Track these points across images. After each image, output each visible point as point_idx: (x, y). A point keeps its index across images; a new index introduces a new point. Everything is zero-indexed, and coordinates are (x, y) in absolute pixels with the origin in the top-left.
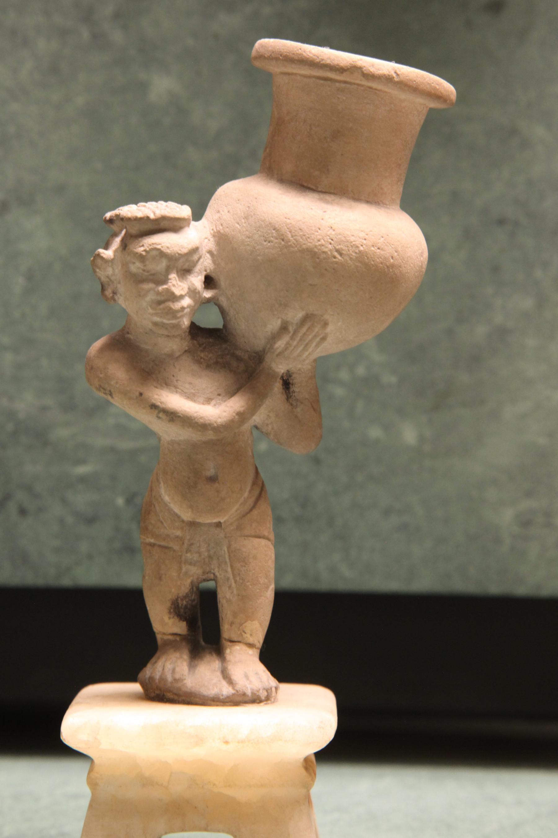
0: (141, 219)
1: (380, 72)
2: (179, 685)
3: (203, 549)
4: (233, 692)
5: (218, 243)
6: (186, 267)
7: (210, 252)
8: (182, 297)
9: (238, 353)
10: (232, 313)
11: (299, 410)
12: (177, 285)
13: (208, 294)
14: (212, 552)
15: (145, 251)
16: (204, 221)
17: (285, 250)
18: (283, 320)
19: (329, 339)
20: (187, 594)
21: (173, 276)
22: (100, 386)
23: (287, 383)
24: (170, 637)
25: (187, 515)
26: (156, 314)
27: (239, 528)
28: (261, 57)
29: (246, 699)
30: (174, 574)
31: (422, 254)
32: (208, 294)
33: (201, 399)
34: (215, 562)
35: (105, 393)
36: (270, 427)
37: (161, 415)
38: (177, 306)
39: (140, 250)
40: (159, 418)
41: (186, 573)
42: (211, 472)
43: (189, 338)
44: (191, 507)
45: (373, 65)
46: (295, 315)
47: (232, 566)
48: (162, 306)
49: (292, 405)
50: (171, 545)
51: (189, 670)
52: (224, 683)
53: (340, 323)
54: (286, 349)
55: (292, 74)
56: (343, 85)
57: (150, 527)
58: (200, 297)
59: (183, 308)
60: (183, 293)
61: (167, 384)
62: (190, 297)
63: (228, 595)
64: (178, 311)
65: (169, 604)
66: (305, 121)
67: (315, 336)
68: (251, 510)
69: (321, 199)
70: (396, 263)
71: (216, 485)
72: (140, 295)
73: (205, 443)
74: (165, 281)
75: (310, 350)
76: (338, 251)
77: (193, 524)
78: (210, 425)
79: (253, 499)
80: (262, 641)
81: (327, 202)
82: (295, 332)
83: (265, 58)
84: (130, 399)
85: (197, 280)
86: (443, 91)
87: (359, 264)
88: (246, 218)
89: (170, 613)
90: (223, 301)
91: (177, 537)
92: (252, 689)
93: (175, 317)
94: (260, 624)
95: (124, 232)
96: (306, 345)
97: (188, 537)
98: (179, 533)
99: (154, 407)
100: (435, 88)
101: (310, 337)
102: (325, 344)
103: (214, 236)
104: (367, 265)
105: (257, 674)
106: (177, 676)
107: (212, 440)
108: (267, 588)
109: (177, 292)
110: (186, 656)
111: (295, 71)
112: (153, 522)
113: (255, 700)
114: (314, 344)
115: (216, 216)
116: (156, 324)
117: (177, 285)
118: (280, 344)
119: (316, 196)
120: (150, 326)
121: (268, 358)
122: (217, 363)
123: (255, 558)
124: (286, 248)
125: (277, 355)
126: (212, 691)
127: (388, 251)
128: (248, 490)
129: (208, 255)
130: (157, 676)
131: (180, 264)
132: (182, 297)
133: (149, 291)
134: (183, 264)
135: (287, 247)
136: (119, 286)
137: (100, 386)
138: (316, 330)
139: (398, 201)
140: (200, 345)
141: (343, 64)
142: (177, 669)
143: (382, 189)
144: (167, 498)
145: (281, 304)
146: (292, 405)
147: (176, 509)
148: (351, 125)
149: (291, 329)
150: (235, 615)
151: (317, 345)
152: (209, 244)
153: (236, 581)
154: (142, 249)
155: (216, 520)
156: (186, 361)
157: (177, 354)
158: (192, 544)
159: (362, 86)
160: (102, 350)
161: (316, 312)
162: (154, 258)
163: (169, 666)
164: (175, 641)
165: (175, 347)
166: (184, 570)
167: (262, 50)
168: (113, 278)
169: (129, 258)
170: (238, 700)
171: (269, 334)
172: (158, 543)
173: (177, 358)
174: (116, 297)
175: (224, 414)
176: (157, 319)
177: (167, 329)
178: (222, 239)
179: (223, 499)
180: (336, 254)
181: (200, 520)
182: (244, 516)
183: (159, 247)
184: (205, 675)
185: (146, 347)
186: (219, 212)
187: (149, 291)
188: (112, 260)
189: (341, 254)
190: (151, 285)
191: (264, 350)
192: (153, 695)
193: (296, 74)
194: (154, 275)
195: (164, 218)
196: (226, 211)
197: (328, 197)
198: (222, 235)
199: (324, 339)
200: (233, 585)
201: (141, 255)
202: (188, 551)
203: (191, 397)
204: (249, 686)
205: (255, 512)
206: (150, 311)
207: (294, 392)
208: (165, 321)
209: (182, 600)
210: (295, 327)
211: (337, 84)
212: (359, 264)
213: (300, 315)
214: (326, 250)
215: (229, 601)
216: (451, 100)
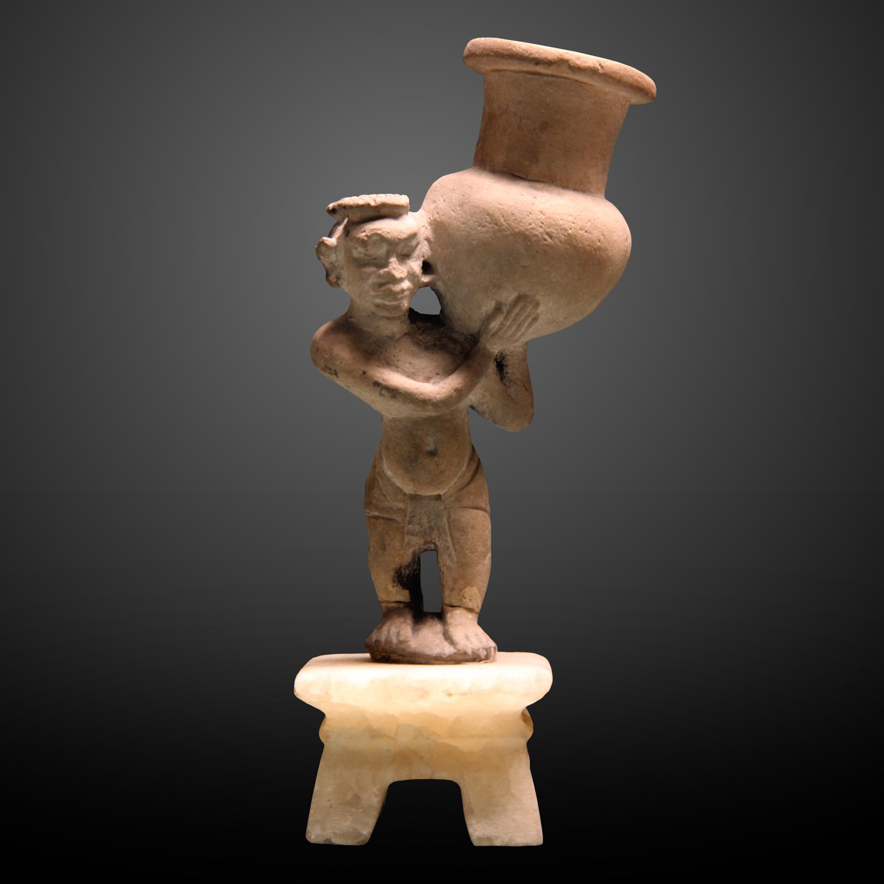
0: (362, 206)
1: (586, 65)
2: (404, 646)
3: (424, 521)
4: (455, 651)
5: (435, 231)
6: (405, 252)
7: (427, 239)
8: (401, 280)
9: (455, 336)
10: (448, 297)
11: (512, 390)
12: (397, 269)
13: (426, 279)
14: (432, 523)
15: (366, 236)
16: (421, 211)
17: (499, 234)
18: (497, 301)
19: (540, 321)
20: (410, 563)
21: (393, 260)
22: (326, 366)
23: (501, 365)
24: (394, 605)
25: (409, 489)
26: (377, 296)
27: (458, 500)
28: (472, 55)
29: (467, 657)
30: (397, 544)
31: (626, 240)
32: (426, 279)
33: (421, 378)
34: (435, 532)
35: (330, 373)
36: (485, 406)
37: (383, 392)
38: (397, 288)
39: (362, 235)
40: (381, 395)
41: (409, 543)
42: (431, 447)
43: (408, 322)
44: (413, 480)
45: (579, 58)
46: (508, 296)
47: (451, 535)
48: (383, 288)
49: (505, 385)
50: (394, 517)
51: (413, 633)
52: (446, 644)
53: (551, 304)
54: (500, 329)
55: (502, 70)
56: (551, 79)
57: (374, 501)
58: (419, 280)
59: (403, 291)
60: (403, 276)
61: (389, 364)
62: (409, 280)
63: (448, 563)
64: (398, 293)
65: (392, 573)
66: (515, 114)
67: (527, 317)
68: (469, 483)
69: (531, 187)
70: (602, 246)
71: (436, 459)
72: (363, 278)
73: (424, 419)
74: (386, 264)
75: (523, 330)
76: (548, 234)
77: (414, 498)
78: (430, 400)
79: (471, 473)
80: (480, 607)
81: (537, 189)
82: (509, 312)
83: (477, 55)
84: (354, 377)
85: (416, 265)
86: (644, 84)
87: (568, 247)
88: (461, 205)
89: (394, 581)
90: (440, 285)
91: (400, 509)
92: (472, 649)
93: (396, 299)
94: (479, 590)
95: (346, 221)
96: (519, 325)
97: (410, 510)
98: (401, 505)
99: (377, 384)
100: (637, 81)
101: (523, 317)
102: (536, 325)
103: (431, 224)
104: (575, 247)
105: (476, 635)
106: (402, 638)
107: (431, 417)
108: (485, 556)
109: (398, 275)
110: (409, 621)
111: (505, 67)
112: (376, 496)
113: (475, 658)
114: (526, 324)
115: (433, 206)
116: (378, 306)
117: (397, 269)
118: (494, 325)
119: (526, 184)
120: (373, 308)
121: (483, 340)
122: (435, 345)
123: (473, 527)
124: (499, 231)
125: (492, 335)
126: (435, 651)
127: (596, 234)
128: (465, 465)
129: (426, 242)
130: (383, 639)
131: (400, 248)
132: (401, 280)
133: (370, 274)
134: (403, 248)
135: (500, 231)
136: (342, 271)
137: (326, 366)
138: (528, 310)
139: (603, 191)
140: (419, 329)
141: (550, 57)
142: (402, 632)
143: (588, 178)
144: (389, 473)
145: (495, 286)
146: (505, 385)
147: (398, 483)
148: (558, 116)
149: (505, 309)
150: (455, 581)
151: (529, 326)
152: (425, 232)
153: (455, 550)
154: (364, 234)
155: (435, 493)
156: (406, 343)
157: (398, 336)
158: (413, 517)
159: (568, 79)
160: (327, 333)
161: (527, 293)
162: (375, 243)
163: (394, 630)
164: (399, 608)
165: (395, 330)
166: (406, 541)
167: (473, 49)
168: (337, 264)
169: (351, 244)
170: (460, 658)
171: (484, 315)
172: (382, 515)
173: (398, 340)
174: (340, 282)
175: (443, 390)
176: (378, 301)
177: (388, 310)
178: (438, 226)
179: (442, 472)
180: (546, 237)
181: (423, 492)
182: (462, 489)
183: (379, 232)
184: (428, 638)
185: (369, 330)
186: (435, 202)
187: (370, 274)
188: (335, 248)
189: (551, 237)
190: (372, 269)
191: (479, 332)
192: (379, 657)
193: (506, 70)
194: (375, 259)
195: (384, 205)
196: (442, 201)
197: (537, 185)
198: (439, 222)
199: (535, 319)
200: (453, 553)
201: (363, 240)
202: (410, 523)
203: (412, 375)
204: (470, 646)
205: (473, 485)
206: (373, 293)
207: (507, 373)
208: (387, 303)
209: (405, 569)
210: (508, 307)
211: (545, 78)
212: (568, 247)
213: (513, 296)
214: (536, 233)
215: (449, 568)
216: (652, 94)
